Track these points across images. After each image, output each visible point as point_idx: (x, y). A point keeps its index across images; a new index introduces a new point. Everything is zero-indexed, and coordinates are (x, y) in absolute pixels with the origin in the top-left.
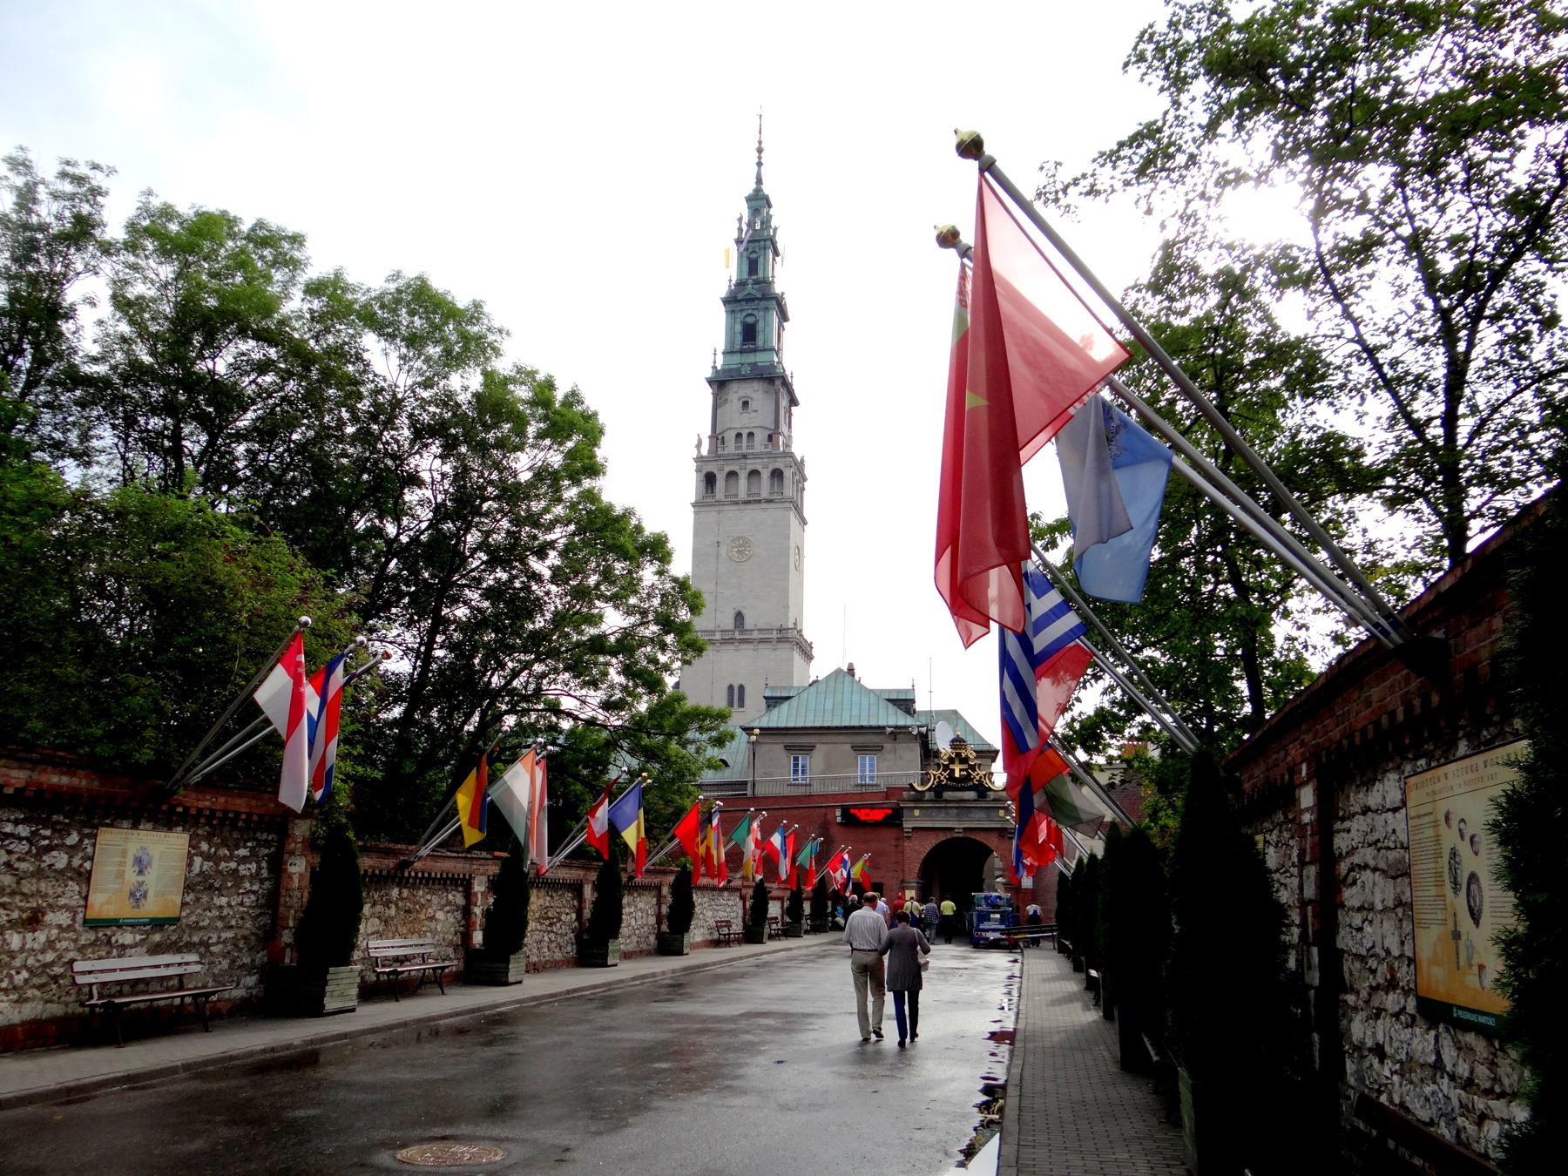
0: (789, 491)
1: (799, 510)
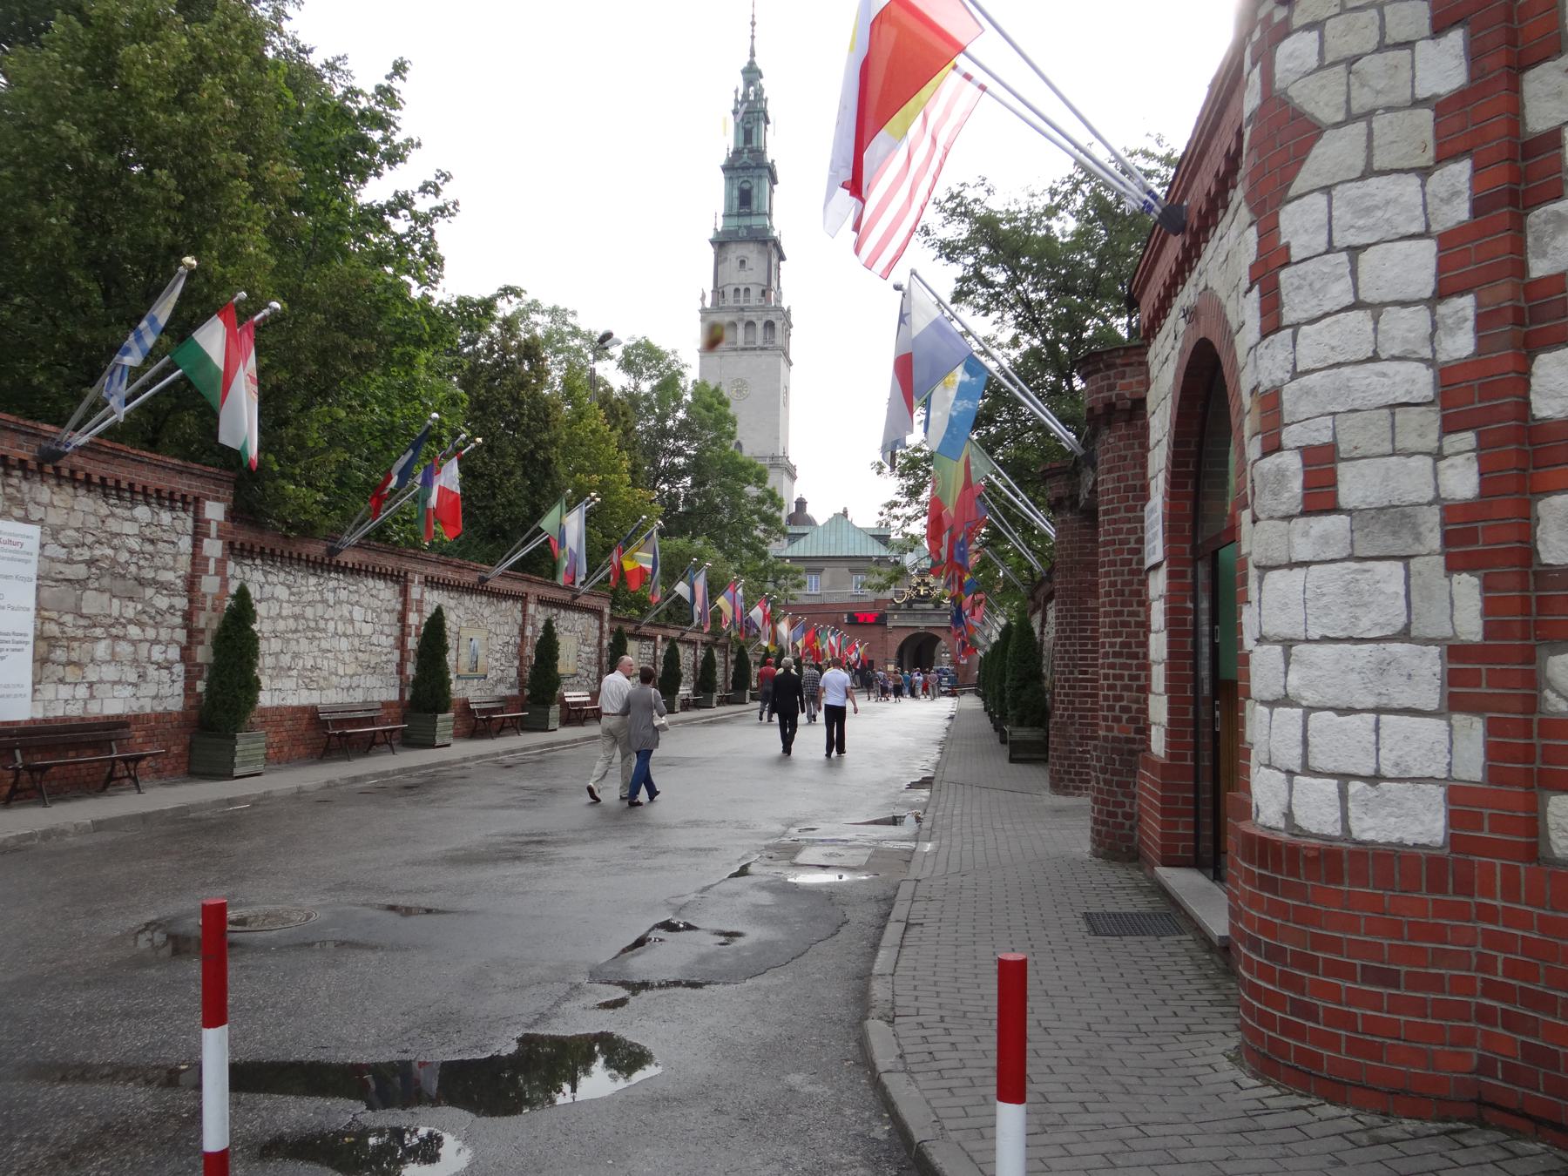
0: (779, 341)
1: (786, 354)
